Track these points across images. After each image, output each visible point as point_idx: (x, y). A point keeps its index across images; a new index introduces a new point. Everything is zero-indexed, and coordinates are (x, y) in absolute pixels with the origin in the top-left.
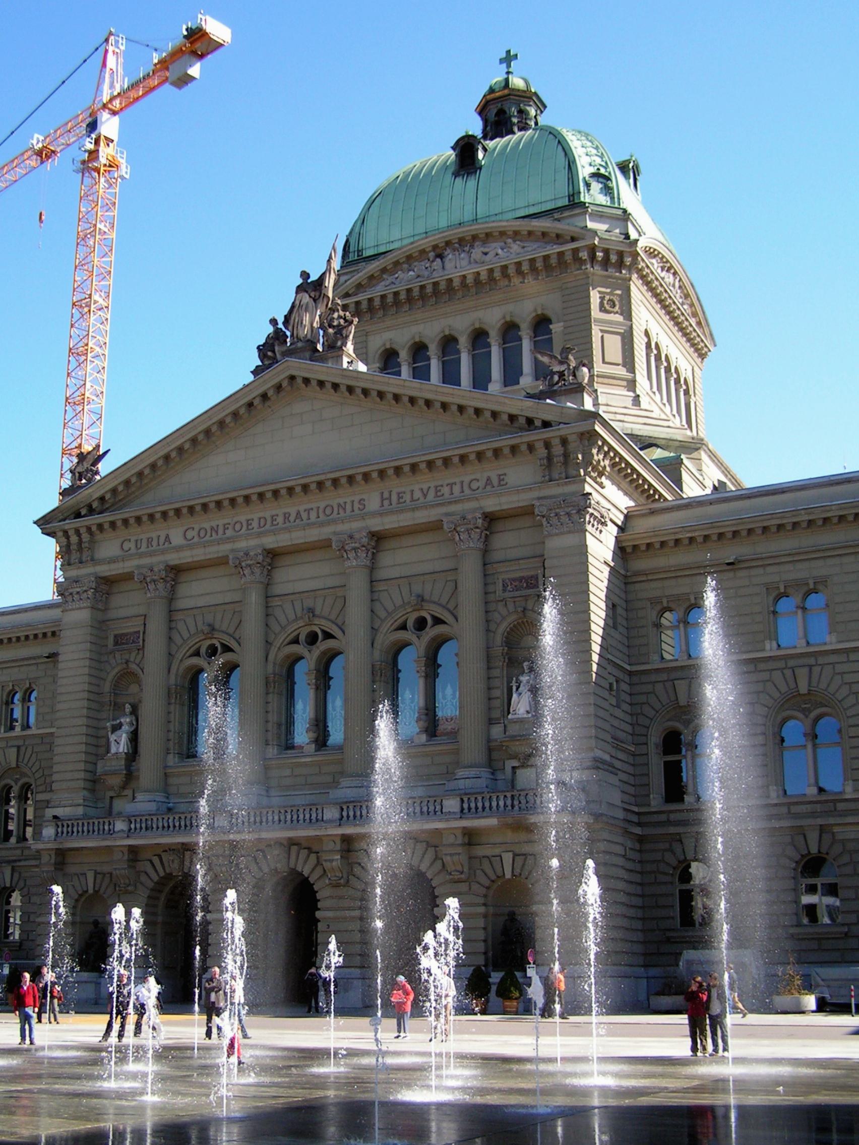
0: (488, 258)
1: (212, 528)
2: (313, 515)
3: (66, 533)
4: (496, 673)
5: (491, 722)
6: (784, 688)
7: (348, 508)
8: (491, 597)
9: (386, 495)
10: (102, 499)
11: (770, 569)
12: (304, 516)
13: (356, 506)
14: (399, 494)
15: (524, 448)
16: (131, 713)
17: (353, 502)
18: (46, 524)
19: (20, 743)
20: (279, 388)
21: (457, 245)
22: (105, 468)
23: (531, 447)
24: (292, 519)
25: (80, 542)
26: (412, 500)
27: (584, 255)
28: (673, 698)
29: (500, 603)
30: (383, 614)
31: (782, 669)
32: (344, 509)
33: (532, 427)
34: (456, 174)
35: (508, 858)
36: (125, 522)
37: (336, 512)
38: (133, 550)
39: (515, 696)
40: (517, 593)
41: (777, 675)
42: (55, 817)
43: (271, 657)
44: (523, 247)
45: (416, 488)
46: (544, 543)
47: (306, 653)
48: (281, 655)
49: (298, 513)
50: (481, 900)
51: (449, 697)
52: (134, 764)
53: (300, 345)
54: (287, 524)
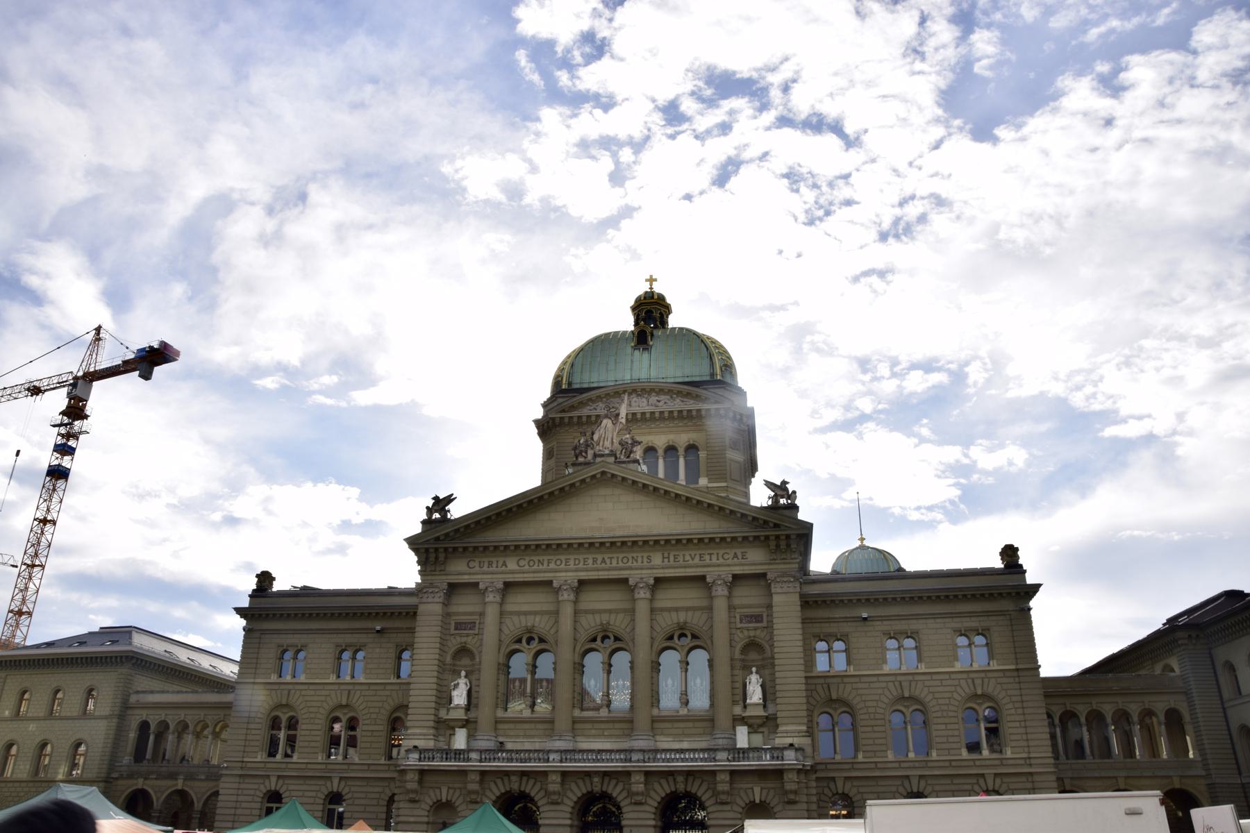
0: (661, 404)
1: (539, 561)
2: (614, 562)
4: (736, 672)
5: (735, 703)
7: (640, 560)
8: (733, 626)
9: (666, 555)
10: (457, 531)
11: (885, 623)
12: (608, 561)
13: (645, 560)
15: (762, 538)
16: (466, 677)
17: (642, 557)
18: (413, 542)
19: (350, 687)
20: (593, 477)
22: (456, 511)
23: (767, 538)
24: (599, 562)
25: (437, 558)
26: (684, 561)
28: (828, 694)
29: (738, 631)
30: (658, 629)
31: (893, 682)
32: (637, 561)
33: (765, 526)
34: (635, 348)
35: (757, 790)
37: (630, 561)
38: (477, 569)
39: (750, 688)
40: (750, 625)
41: (891, 684)
42: (415, 747)
43: (578, 649)
44: (682, 401)
45: (687, 553)
46: (771, 595)
48: (583, 649)
49: (604, 559)
51: (698, 685)
53: (607, 452)
54: (595, 566)
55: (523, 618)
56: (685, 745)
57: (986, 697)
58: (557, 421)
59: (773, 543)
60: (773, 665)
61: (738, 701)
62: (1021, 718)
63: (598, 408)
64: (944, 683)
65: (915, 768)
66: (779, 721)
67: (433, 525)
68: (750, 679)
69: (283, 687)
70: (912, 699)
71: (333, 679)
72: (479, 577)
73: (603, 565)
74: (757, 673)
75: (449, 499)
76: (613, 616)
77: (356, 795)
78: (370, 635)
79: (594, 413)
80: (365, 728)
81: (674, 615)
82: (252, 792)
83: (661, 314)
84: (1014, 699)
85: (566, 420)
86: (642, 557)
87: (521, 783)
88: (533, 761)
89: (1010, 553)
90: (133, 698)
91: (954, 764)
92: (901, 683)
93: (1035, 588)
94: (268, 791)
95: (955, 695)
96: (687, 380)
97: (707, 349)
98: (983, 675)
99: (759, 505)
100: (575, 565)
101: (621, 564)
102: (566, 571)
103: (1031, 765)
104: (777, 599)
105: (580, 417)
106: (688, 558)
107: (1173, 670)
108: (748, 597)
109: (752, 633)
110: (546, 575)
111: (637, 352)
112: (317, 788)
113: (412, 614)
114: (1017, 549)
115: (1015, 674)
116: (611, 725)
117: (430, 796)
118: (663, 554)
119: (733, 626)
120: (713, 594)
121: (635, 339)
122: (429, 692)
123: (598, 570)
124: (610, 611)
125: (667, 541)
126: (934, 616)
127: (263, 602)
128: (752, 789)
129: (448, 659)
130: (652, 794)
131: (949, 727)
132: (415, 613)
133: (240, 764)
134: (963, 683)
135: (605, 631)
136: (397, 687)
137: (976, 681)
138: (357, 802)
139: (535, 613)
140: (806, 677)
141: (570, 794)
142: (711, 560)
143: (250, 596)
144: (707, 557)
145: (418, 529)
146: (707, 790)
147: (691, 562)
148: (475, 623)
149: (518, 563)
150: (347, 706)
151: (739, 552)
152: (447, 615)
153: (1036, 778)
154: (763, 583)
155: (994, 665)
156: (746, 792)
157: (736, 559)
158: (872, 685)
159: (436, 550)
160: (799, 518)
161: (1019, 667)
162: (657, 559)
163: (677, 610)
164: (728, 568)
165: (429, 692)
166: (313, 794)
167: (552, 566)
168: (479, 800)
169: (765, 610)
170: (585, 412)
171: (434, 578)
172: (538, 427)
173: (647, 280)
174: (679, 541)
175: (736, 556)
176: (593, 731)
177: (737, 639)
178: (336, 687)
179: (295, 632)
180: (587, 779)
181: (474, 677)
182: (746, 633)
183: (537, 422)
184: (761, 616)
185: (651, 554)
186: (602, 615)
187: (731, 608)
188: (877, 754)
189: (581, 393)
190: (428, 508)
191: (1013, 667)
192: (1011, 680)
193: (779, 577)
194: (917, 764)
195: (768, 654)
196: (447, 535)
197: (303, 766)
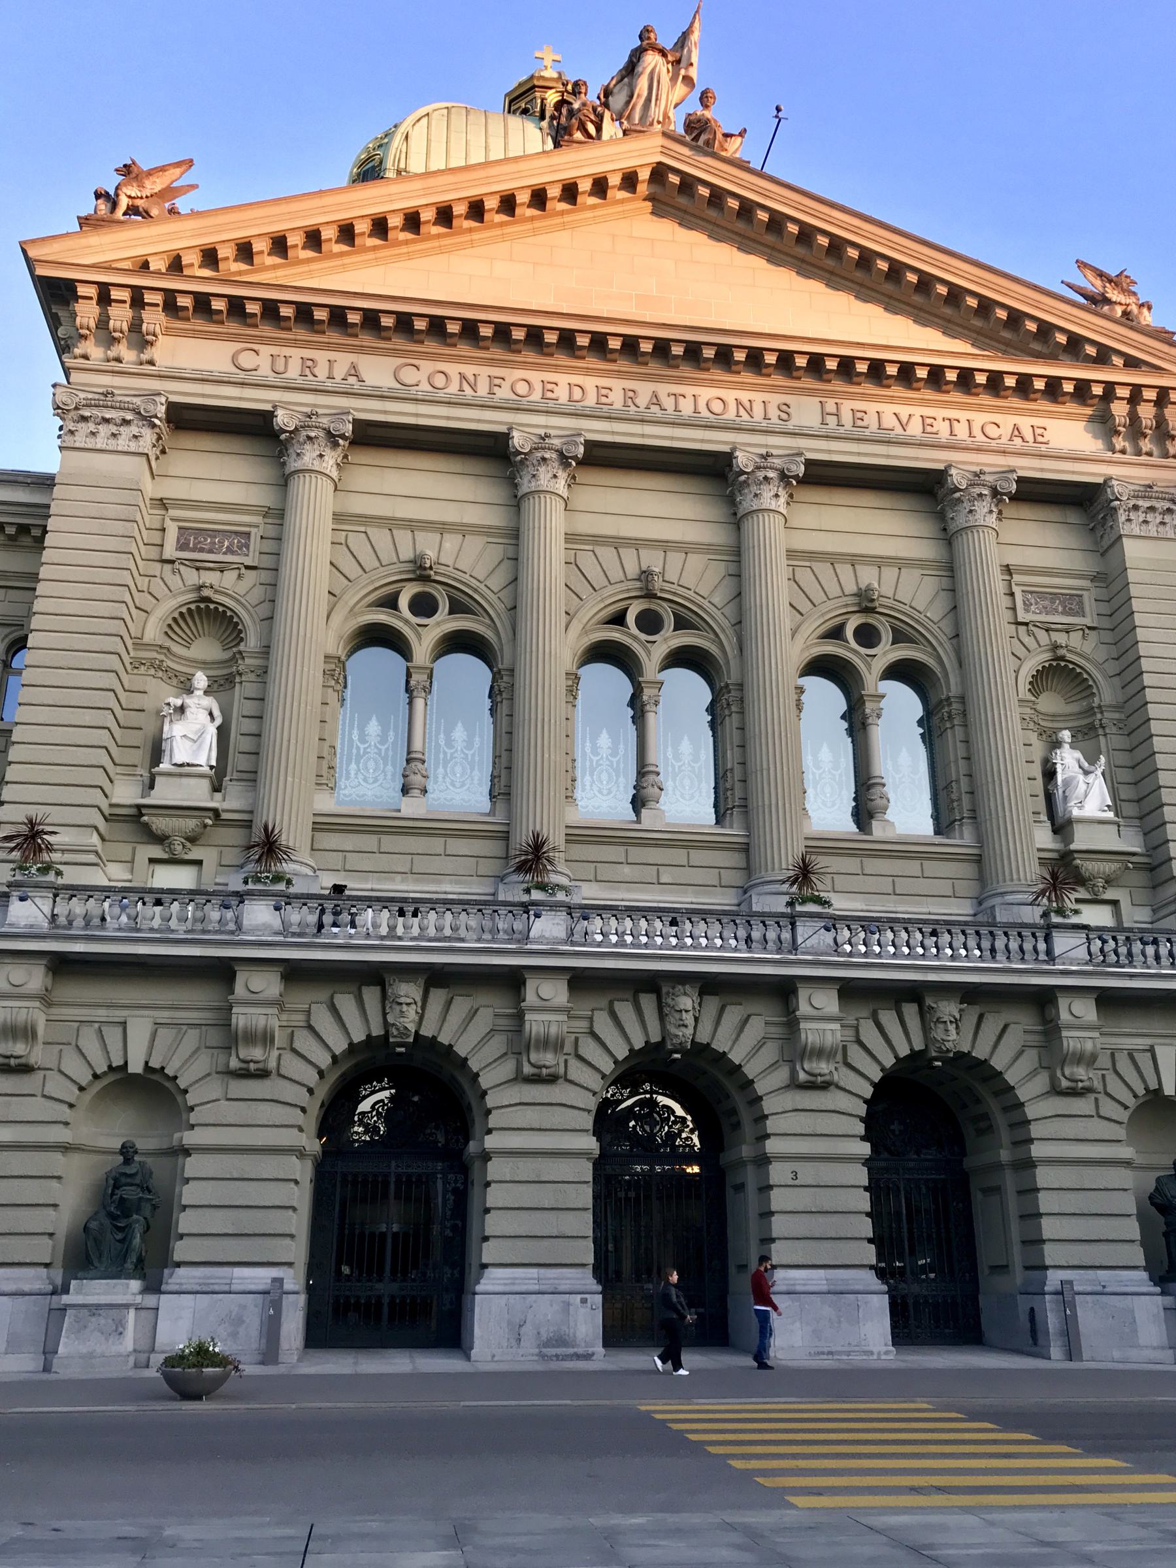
1: (463, 377)
3: (104, 297)
12: (669, 403)
15: (1097, 390)
16: (206, 693)
29: (1022, 629)
49: (655, 395)
50: (1120, 1132)
52: (218, 796)
59: (1120, 409)
61: (1039, 813)
74: (1073, 746)
87: (423, 1008)
104: (1133, 550)
109: (1061, 638)
116: (679, 856)
120: (952, 527)
124: (664, 545)
128: (1151, 1050)
129: (153, 632)
135: (650, 595)
139: (443, 528)
146: (1021, 1053)
148: (248, 534)
151: (1025, 423)
154: (1073, 516)
167: (503, 393)
176: (627, 869)
180: (648, 1002)
182: (1042, 635)
190: (98, 195)
195: (1107, 693)
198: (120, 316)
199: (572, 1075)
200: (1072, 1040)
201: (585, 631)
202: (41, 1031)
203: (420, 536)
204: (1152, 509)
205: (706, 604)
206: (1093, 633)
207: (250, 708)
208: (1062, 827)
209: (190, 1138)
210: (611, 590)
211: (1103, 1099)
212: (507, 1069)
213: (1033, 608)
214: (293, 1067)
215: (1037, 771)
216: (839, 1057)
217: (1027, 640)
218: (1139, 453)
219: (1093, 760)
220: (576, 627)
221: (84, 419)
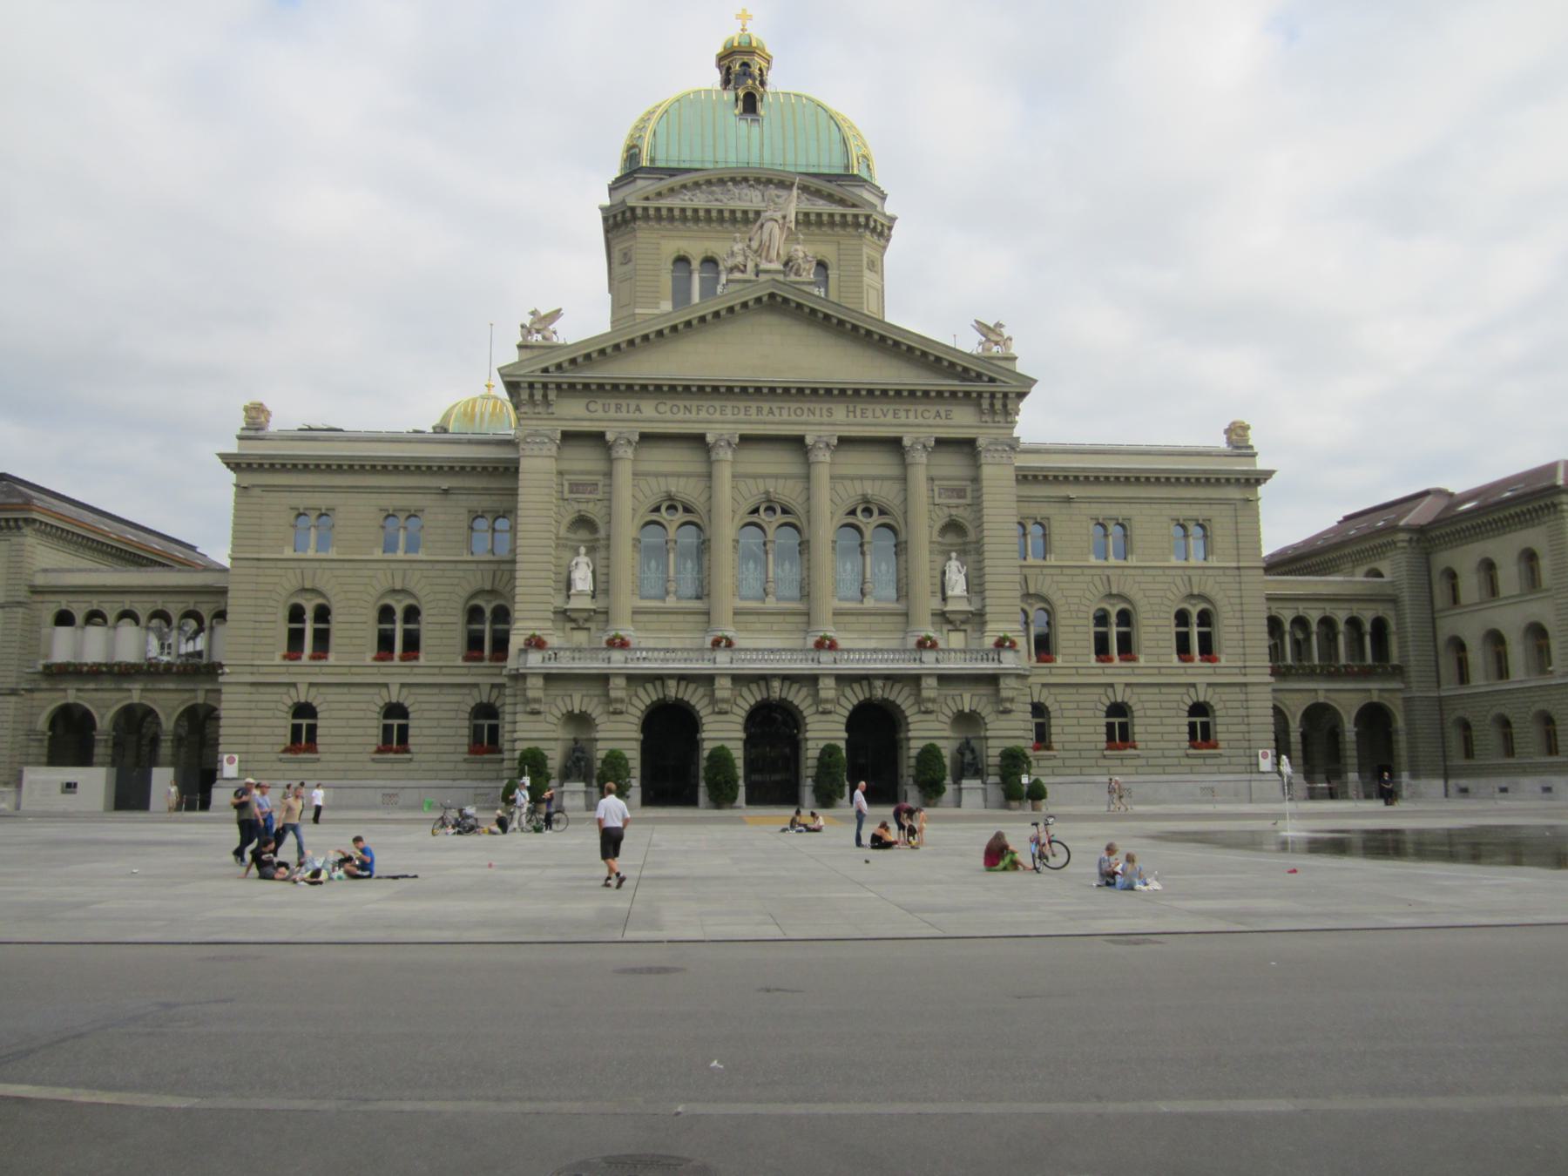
1: (685, 407)
2: (785, 412)
6: (1101, 588)
7: (817, 412)
9: (851, 409)
10: (573, 361)
12: (776, 412)
14: (862, 410)
15: (974, 395)
17: (821, 409)
20: (758, 300)
21: (752, 182)
23: (980, 394)
24: (766, 411)
27: (862, 220)
32: (814, 414)
35: (967, 697)
36: (601, 386)
37: (806, 411)
41: (1096, 578)
44: (808, 200)
45: (878, 408)
47: (764, 525)
49: (771, 408)
54: (760, 417)
55: (662, 480)
56: (873, 644)
57: (1202, 597)
58: (639, 212)
59: (985, 404)
60: (979, 551)
62: (1239, 622)
63: (695, 200)
64: (1158, 579)
65: (1120, 675)
66: (988, 617)
67: (536, 352)
68: (950, 567)
69: (303, 564)
70: (1121, 597)
71: (378, 554)
72: (605, 424)
73: (771, 417)
74: (957, 559)
75: (556, 315)
76: (781, 482)
77: (425, 706)
78: (429, 496)
79: (688, 204)
80: (430, 619)
81: (857, 484)
82: (272, 705)
83: (760, 70)
84: (1232, 600)
85: (652, 212)
86: (821, 409)
88: (694, 661)
89: (1237, 435)
90: (40, 580)
91: (1163, 671)
92: (1108, 577)
93: (1268, 474)
94: (295, 704)
95: (1169, 595)
96: (812, 170)
97: (839, 129)
98: (1200, 572)
99: (968, 351)
100: (733, 414)
101: (793, 418)
102: (723, 422)
103: (1245, 675)
104: (987, 471)
105: (670, 210)
106: (878, 413)
107: (1380, 575)
108: (952, 466)
109: (954, 512)
110: (696, 425)
111: (743, 124)
112: (368, 698)
113: (513, 470)
114: (1246, 428)
115: (1236, 572)
116: (781, 618)
117: (556, 706)
118: (848, 407)
119: (931, 501)
121: (740, 104)
122: (543, 574)
123: (765, 423)
124: (776, 477)
125: (857, 392)
126: (1150, 501)
127: (257, 449)
128: (961, 695)
129: (563, 532)
130: (843, 700)
131: (1160, 629)
132: (517, 469)
133: (249, 669)
134: (1178, 580)
135: (770, 501)
136: (473, 566)
137: (1193, 579)
138: (427, 714)
140: (1021, 567)
141: (740, 701)
142: (907, 418)
143: (240, 438)
144: (902, 414)
145: (512, 356)
147: (882, 420)
148: (597, 484)
149: (660, 413)
150: (403, 591)
151: (942, 409)
152: (561, 473)
153: (1250, 689)
155: (1213, 561)
156: (953, 698)
157: (938, 418)
158: (1076, 579)
159: (545, 386)
160: (1018, 371)
161: (1242, 564)
162: (840, 412)
163: (861, 478)
164: (928, 430)
165: (543, 574)
166: (363, 706)
167: (703, 415)
168: (624, 709)
169: (968, 483)
170: (676, 202)
171: (539, 422)
172: (605, 220)
173: (738, 17)
174: (870, 392)
175: (938, 414)
176: (759, 626)
177: (934, 517)
178: (384, 565)
179: (314, 489)
180: (762, 684)
181: (601, 554)
182: (946, 510)
183: (603, 209)
184: (965, 490)
185: (832, 406)
186: (767, 480)
187: (932, 479)
188: (1079, 658)
189: (671, 176)
190: (523, 326)
191: (1234, 564)
192: (1231, 579)
193: (990, 444)
194: (1122, 671)
195: (972, 536)
196: (559, 367)
197: (345, 670)
198: (538, 396)
199: (734, 711)
200: (926, 693)
201: (742, 519)
202: (543, 700)
203: (670, 479)
204: (997, 450)
205: (795, 504)
206: (969, 509)
207: (604, 562)
208: (944, 599)
209: (598, 735)
210: (752, 500)
211: (940, 714)
212: (709, 710)
213: (943, 496)
214: (632, 710)
215: (938, 574)
216: (836, 701)
217: (938, 512)
218: (994, 422)
219: (963, 568)
220: (737, 518)
221: (528, 443)
